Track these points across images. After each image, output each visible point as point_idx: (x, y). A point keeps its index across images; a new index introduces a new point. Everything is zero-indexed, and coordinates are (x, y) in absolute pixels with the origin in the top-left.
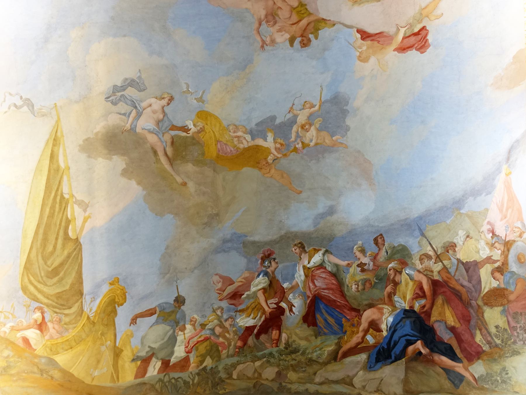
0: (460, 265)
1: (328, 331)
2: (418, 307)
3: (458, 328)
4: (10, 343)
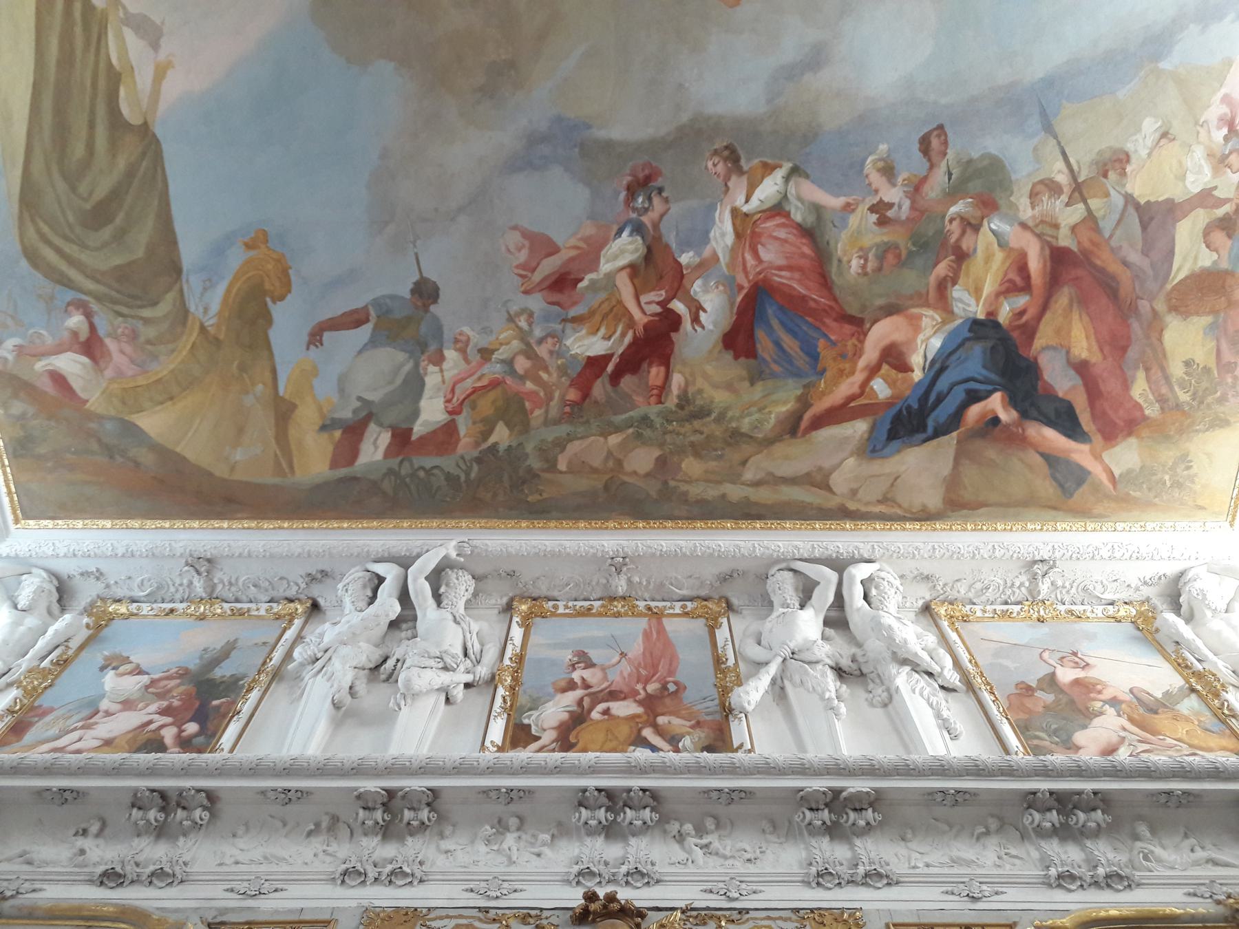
0: (1131, 210)
1: (781, 369)
2: (1009, 313)
3: (1095, 364)
4: (22, 387)
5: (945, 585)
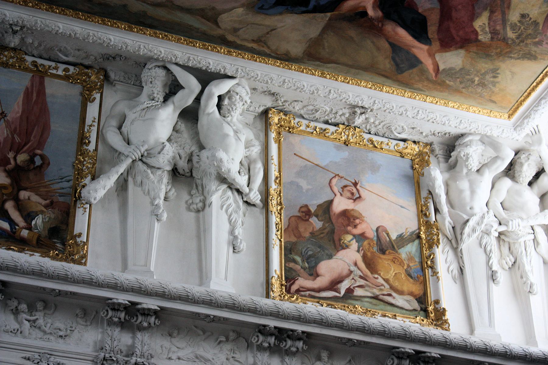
5: (285, 101)
